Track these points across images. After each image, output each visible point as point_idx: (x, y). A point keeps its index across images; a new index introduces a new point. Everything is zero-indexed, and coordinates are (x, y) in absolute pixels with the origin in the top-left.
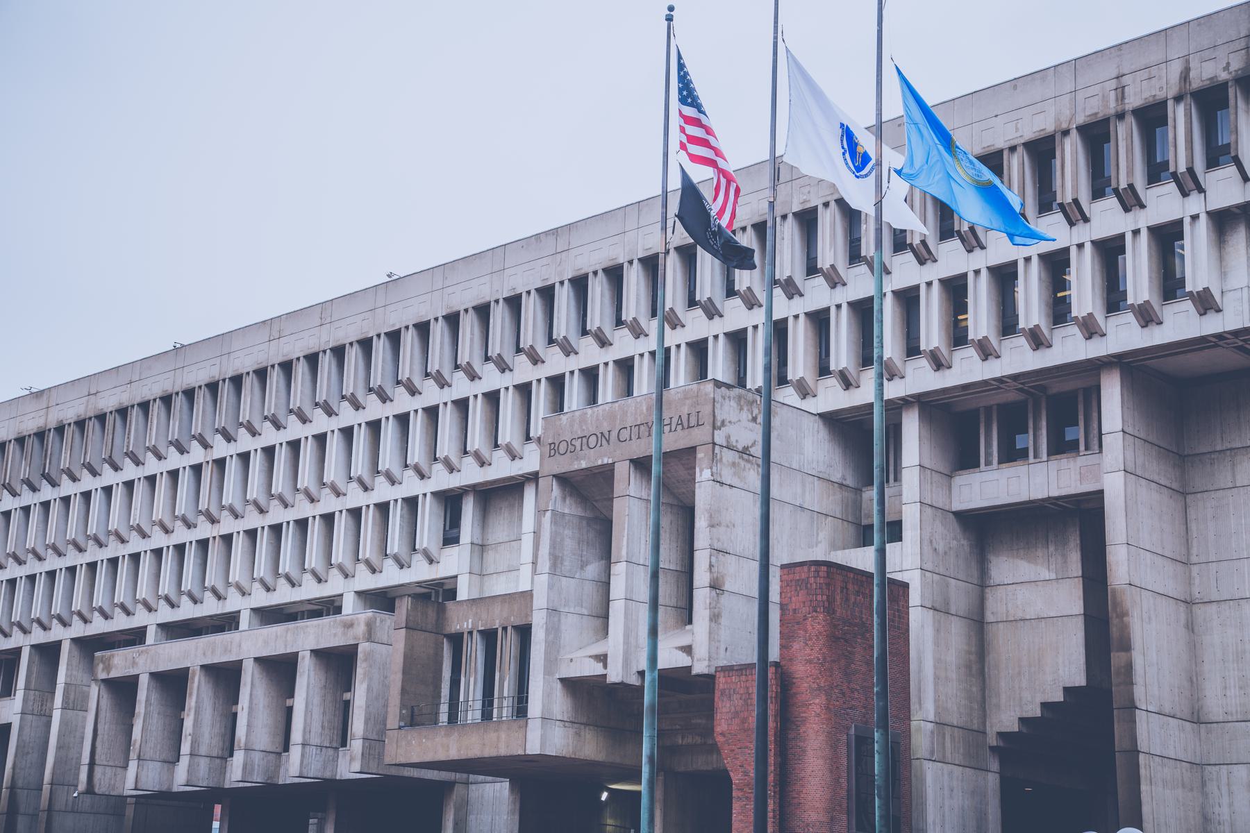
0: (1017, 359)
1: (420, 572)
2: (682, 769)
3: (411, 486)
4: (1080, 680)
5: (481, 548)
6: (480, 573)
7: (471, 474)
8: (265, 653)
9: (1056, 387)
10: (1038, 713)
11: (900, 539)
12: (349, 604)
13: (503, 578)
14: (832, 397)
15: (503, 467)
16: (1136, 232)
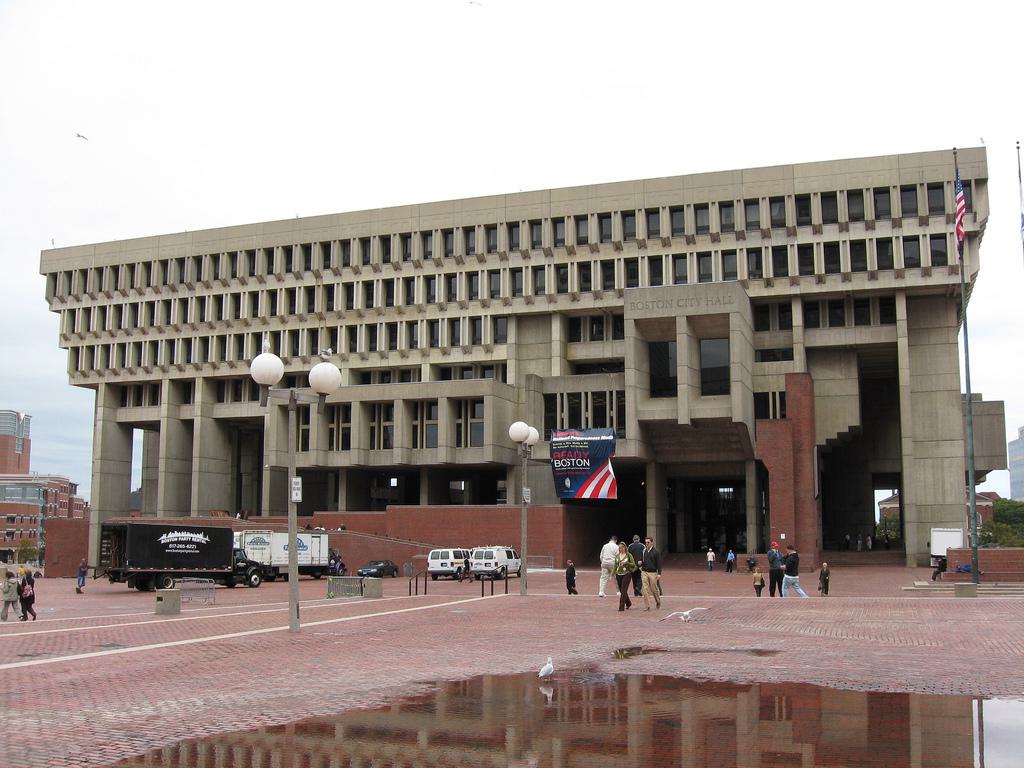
0: (860, 283)
1: (478, 356)
2: (661, 461)
3: (475, 310)
4: (855, 421)
5: (518, 345)
6: (518, 360)
7: (519, 307)
8: (411, 397)
9: (858, 296)
10: (836, 437)
11: (792, 359)
12: (426, 372)
13: (534, 363)
14: (757, 290)
15: (541, 306)
16: (925, 236)
